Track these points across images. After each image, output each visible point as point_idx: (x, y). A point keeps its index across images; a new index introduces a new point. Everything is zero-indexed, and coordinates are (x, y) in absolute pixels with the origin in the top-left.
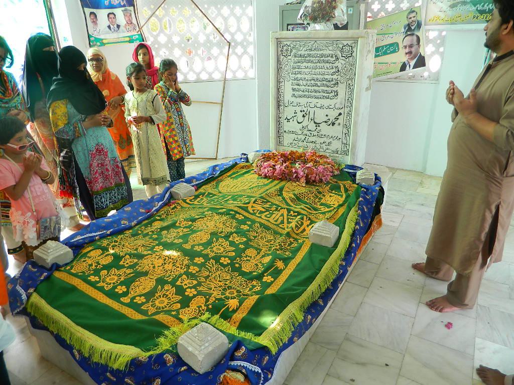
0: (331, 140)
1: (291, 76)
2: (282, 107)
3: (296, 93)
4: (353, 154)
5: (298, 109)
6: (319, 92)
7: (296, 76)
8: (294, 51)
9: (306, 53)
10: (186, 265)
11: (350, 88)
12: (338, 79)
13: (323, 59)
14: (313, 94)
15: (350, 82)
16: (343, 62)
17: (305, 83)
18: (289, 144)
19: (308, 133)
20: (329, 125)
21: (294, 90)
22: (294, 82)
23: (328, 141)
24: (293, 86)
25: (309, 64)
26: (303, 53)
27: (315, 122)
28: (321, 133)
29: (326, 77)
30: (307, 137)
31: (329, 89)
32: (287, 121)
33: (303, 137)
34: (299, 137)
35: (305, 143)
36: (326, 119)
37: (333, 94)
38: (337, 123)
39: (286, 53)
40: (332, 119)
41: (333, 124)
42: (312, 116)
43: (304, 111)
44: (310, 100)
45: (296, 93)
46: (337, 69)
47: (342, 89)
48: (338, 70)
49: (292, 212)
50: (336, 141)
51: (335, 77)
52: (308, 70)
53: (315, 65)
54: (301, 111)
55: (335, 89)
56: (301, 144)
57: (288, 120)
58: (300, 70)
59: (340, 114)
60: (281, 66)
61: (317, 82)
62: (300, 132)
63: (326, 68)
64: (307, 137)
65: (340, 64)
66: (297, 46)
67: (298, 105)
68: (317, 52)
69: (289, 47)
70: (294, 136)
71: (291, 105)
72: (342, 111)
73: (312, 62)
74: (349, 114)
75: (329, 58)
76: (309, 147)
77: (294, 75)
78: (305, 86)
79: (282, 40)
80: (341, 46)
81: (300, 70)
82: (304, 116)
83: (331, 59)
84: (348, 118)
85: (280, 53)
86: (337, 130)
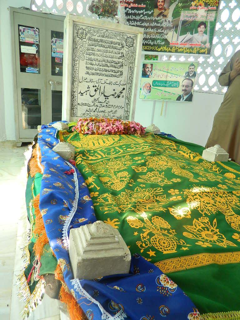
0: (117, 109)
1: (85, 56)
2: (77, 83)
3: (90, 71)
4: (133, 118)
5: (91, 85)
6: (109, 71)
7: (90, 57)
8: (89, 35)
9: (99, 38)
10: (228, 192)
11: (131, 69)
12: (123, 62)
13: (112, 45)
14: (104, 73)
15: (131, 65)
16: (127, 50)
17: (97, 63)
18: (82, 115)
19: (99, 104)
20: (116, 97)
21: (87, 67)
22: (88, 61)
23: (114, 110)
24: (87, 65)
25: (101, 48)
26: (96, 38)
27: (105, 96)
28: (109, 104)
29: (114, 60)
30: (98, 108)
31: (116, 69)
32: (81, 95)
33: (94, 108)
34: (91, 108)
35: (96, 113)
36: (113, 93)
37: (119, 74)
38: (121, 95)
39: (81, 35)
40: (118, 93)
41: (119, 97)
42: (102, 90)
43: (96, 86)
44: (101, 77)
45: (89, 71)
46: (122, 55)
47: (125, 70)
48: (123, 56)
49: (173, 150)
50: (120, 109)
51: (121, 60)
52: (100, 52)
53: (106, 49)
54: (94, 86)
55: (120, 69)
56: (92, 113)
57: (82, 94)
58: (93, 52)
59: (124, 89)
60: (76, 46)
61: (107, 64)
62: (92, 104)
63: (114, 53)
64: (98, 108)
65: (124, 51)
66: (91, 31)
67: (91, 81)
68: (108, 39)
69: (85, 31)
70: (86, 108)
71: (86, 80)
72: (125, 87)
73: (104, 46)
74: (130, 89)
75: (117, 45)
76: (99, 116)
77: (88, 56)
78: (97, 66)
79: (78, 23)
80: (126, 37)
81: (93, 52)
82: (96, 91)
83: (118, 46)
84: (129, 91)
85: (76, 35)
86: (121, 101)
